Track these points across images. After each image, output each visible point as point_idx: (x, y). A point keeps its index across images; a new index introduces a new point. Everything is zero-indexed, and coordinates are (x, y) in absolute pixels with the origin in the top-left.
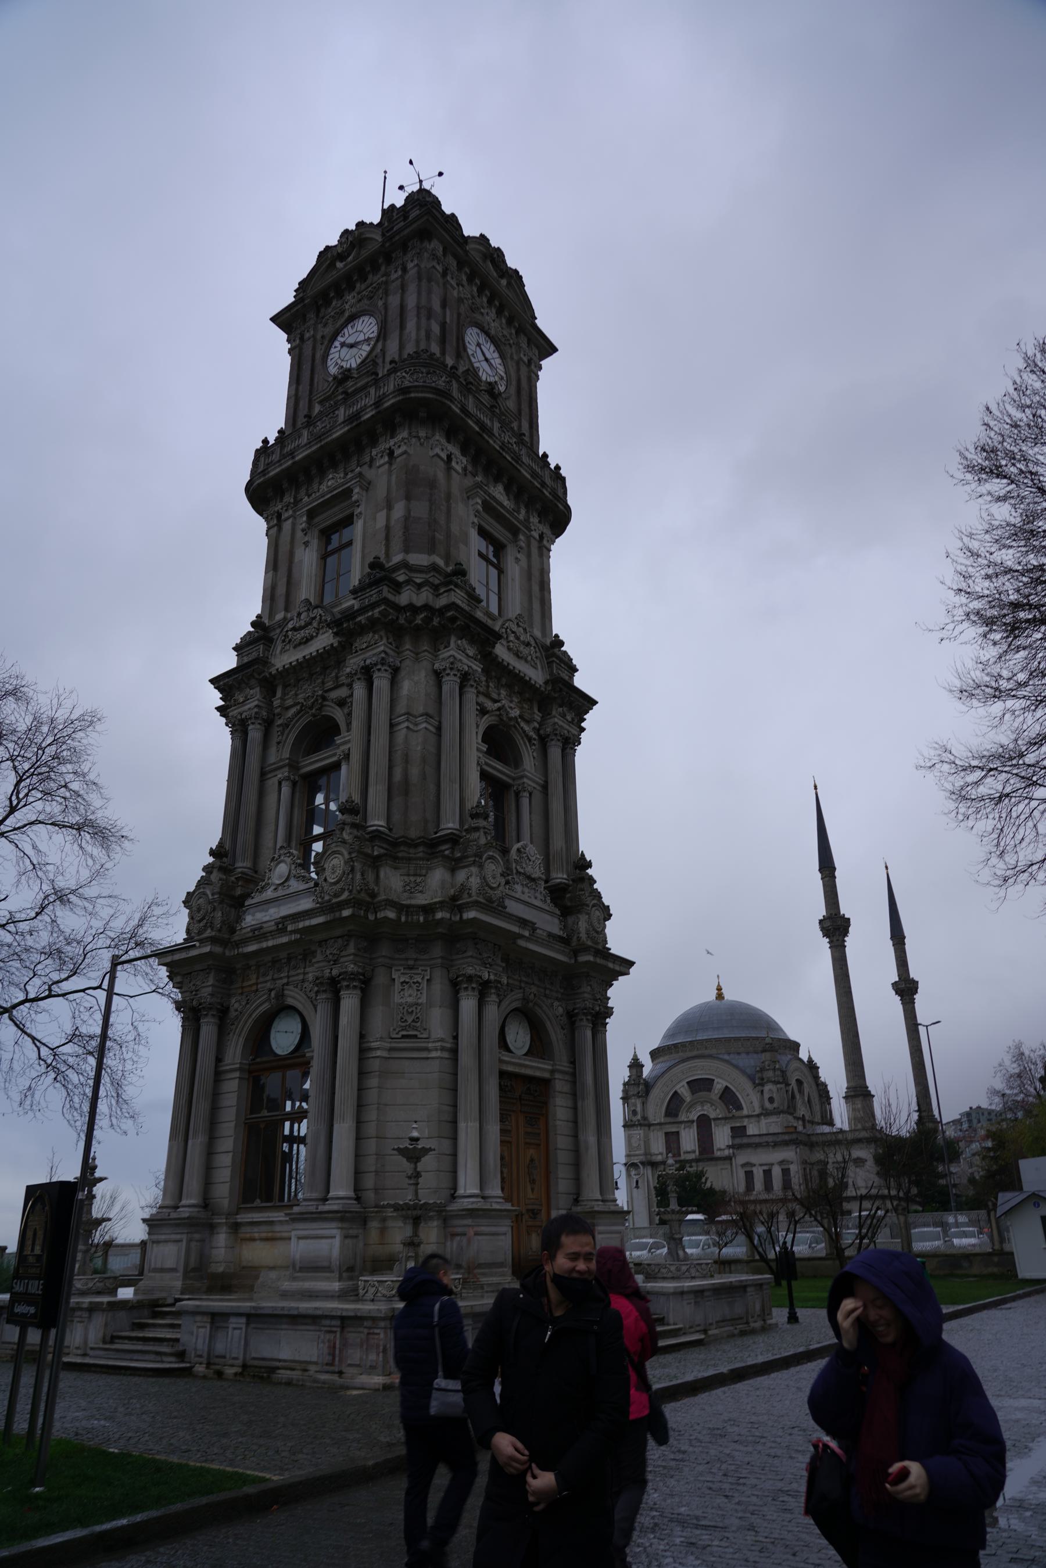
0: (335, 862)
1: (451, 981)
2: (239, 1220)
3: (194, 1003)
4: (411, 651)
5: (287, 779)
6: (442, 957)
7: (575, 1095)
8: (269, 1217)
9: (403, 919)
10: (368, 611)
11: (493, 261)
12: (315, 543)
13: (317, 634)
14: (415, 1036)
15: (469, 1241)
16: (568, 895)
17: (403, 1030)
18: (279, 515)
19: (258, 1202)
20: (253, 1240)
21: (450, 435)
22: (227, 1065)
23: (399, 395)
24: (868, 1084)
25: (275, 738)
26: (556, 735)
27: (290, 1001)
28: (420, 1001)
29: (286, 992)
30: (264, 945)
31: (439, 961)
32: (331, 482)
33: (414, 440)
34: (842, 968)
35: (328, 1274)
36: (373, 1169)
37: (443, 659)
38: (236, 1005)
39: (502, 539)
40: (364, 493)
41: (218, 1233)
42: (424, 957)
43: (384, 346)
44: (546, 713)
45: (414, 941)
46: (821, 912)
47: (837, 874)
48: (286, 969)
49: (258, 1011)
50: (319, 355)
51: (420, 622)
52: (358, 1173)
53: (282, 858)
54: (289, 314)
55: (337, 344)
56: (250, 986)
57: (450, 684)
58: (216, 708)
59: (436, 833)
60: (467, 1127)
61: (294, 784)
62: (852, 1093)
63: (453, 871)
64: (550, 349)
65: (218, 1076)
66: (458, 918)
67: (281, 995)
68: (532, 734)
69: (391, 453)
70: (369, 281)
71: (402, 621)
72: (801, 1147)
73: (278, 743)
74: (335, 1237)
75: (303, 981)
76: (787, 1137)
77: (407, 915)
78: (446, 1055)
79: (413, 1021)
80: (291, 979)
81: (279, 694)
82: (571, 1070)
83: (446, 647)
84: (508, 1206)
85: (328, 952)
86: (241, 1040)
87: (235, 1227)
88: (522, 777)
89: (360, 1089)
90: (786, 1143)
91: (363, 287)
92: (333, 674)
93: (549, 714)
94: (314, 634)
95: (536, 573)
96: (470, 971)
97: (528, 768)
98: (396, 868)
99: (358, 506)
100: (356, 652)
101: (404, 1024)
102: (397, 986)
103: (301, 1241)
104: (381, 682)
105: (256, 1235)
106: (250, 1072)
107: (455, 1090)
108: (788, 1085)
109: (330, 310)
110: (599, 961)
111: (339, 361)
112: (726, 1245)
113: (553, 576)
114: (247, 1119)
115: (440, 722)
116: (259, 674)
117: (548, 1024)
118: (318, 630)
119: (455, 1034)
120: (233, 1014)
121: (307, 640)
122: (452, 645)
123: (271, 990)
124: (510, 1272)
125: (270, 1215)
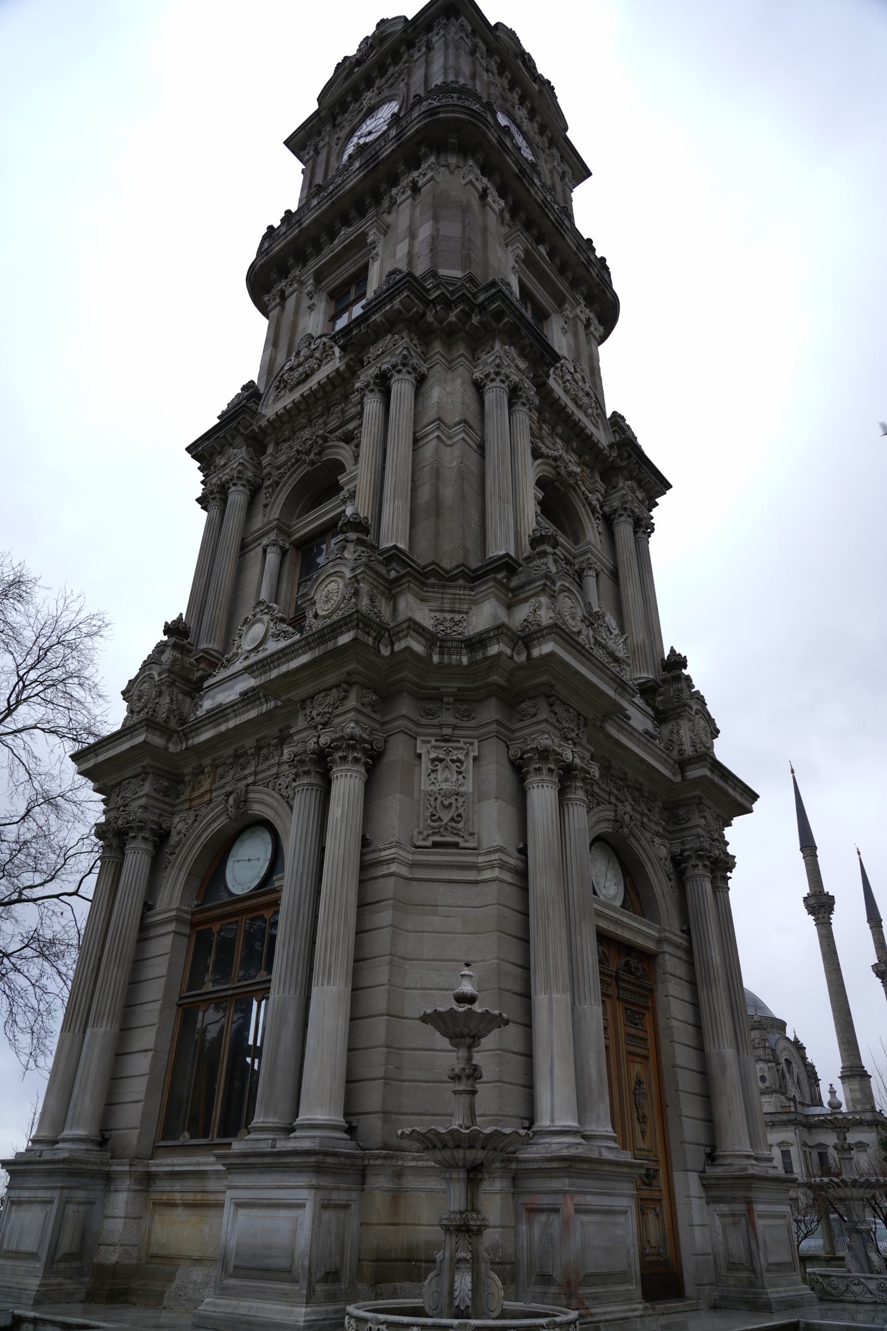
0: (333, 586)
1: (512, 763)
2: (153, 1169)
3: (120, 822)
4: (442, 356)
5: (274, 544)
6: (498, 722)
8: (199, 1164)
9: (436, 659)
10: (385, 305)
11: (524, 62)
13: (320, 366)
14: (455, 845)
15: (566, 1224)
16: (659, 699)
17: (434, 833)
19: (185, 1138)
20: (172, 1205)
21: (486, 170)
22: (158, 914)
23: (425, 118)
24: (864, 1064)
25: (262, 499)
26: (625, 509)
27: (257, 809)
28: (462, 789)
29: (251, 795)
30: (223, 728)
31: (494, 727)
32: (346, 234)
33: (442, 169)
34: (829, 946)
35: (286, 1286)
36: (380, 1072)
38: (180, 826)
39: (544, 303)
40: (382, 237)
41: (116, 1191)
42: (469, 724)
44: (611, 487)
45: (451, 699)
46: (805, 889)
47: (818, 853)
48: (253, 763)
49: (209, 831)
51: (454, 319)
52: (352, 1081)
53: (258, 616)
54: (303, 132)
56: (202, 796)
57: (496, 395)
60: (550, 1000)
61: (284, 553)
62: (848, 1073)
63: (510, 607)
65: (145, 931)
66: (523, 657)
67: (243, 802)
70: (390, 73)
71: (430, 318)
72: (801, 1128)
73: (266, 506)
74: (301, 1206)
75: (277, 776)
76: (784, 1117)
77: (441, 653)
78: (507, 877)
79: (452, 819)
80: (259, 777)
81: (270, 449)
82: (685, 943)
84: (626, 1156)
85: (314, 713)
86: (183, 876)
87: (148, 1179)
88: (585, 553)
89: (360, 932)
90: (785, 1124)
93: (614, 488)
94: (316, 366)
96: (545, 741)
97: (593, 541)
98: (423, 600)
99: (374, 248)
100: (369, 362)
101: (436, 824)
102: (425, 763)
103: (241, 1211)
105: (178, 1197)
106: (193, 925)
107: (525, 940)
108: (778, 1064)
109: (346, 115)
110: (717, 780)
112: (805, 1237)
113: (602, 364)
114: (181, 998)
115: (483, 440)
116: (246, 429)
117: (649, 868)
118: (321, 361)
119: (521, 845)
120: (174, 838)
121: (307, 376)
123: (228, 795)
124: (639, 1292)
125: (201, 1159)
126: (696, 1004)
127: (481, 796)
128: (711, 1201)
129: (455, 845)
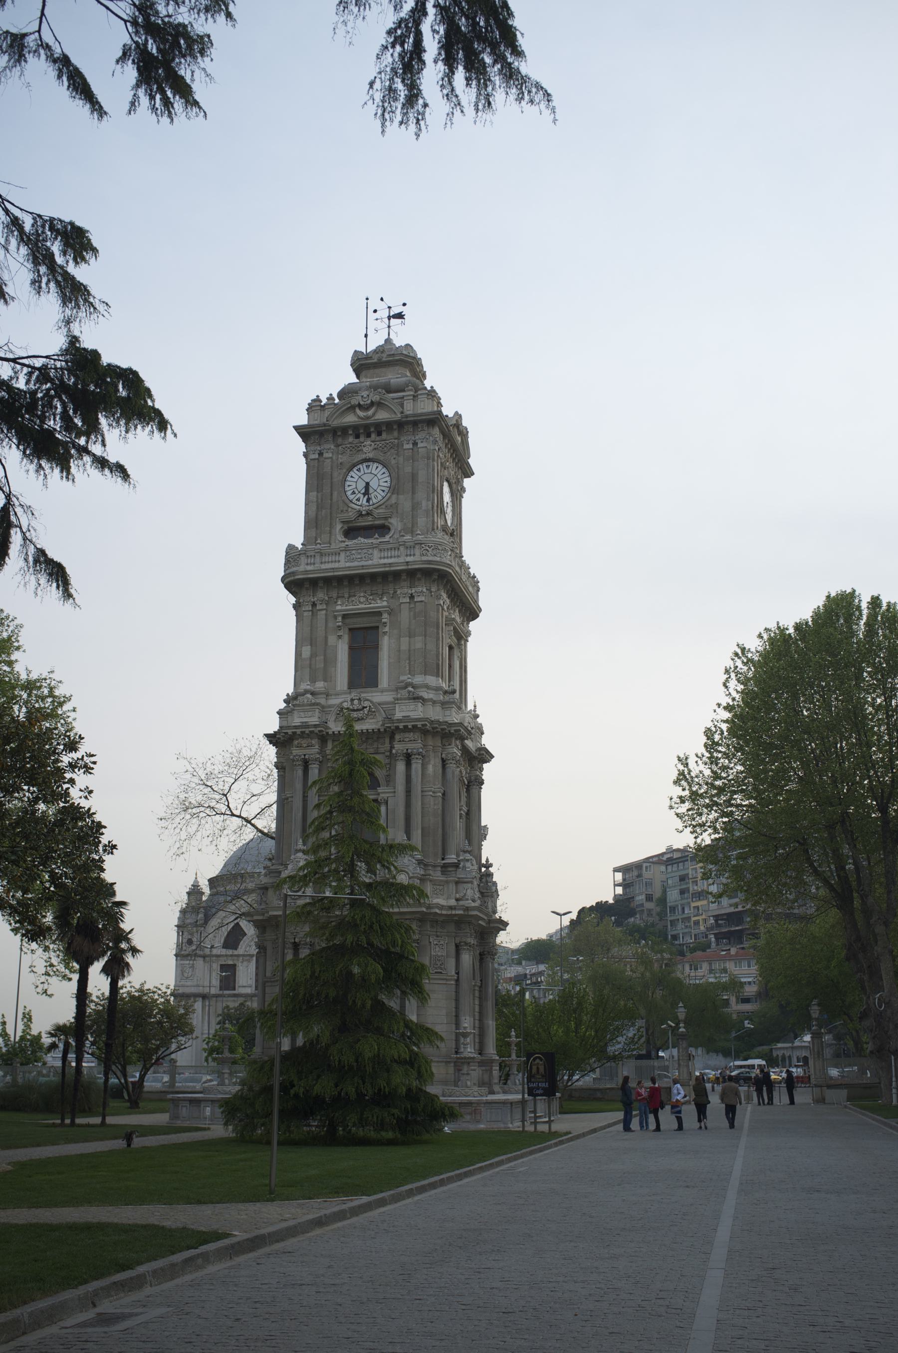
1: (456, 944)
12: (346, 638)
14: (441, 973)
18: (314, 605)
37: (449, 753)
42: (445, 931)
43: (397, 499)
50: (337, 476)
55: (352, 473)
57: (451, 766)
59: (443, 859)
64: (469, 473)
68: (466, 782)
69: (412, 597)
83: (450, 745)
91: (378, 438)
92: (375, 746)
104: (416, 766)
107: (457, 1000)
111: (357, 492)
126: (480, 1006)
127: (448, 956)
129: (441, 973)
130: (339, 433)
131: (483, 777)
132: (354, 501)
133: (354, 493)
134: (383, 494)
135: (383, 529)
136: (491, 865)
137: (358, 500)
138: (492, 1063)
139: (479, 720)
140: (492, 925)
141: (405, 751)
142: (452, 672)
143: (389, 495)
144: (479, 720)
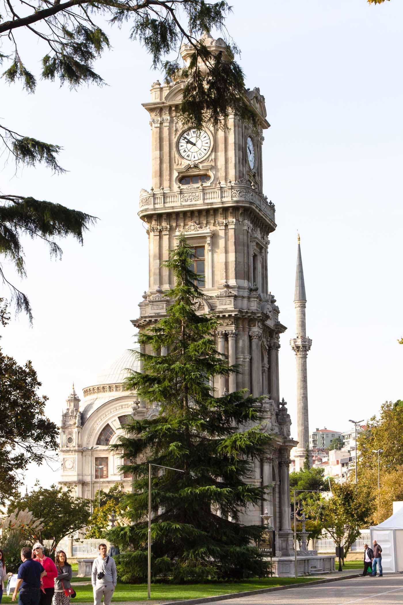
7: (280, 493)
14: (251, 478)
18: (160, 232)
23: (234, 203)
57: (255, 341)
58: (131, 321)
68: (267, 348)
95: (265, 266)
111: (187, 151)
115: (251, 357)
122: (256, 325)
126: (280, 498)
128: (279, 538)
129: (251, 478)
130: (173, 109)
131: (280, 343)
132: (185, 157)
133: (185, 151)
134: (205, 152)
135: (205, 177)
136: (286, 403)
137: (188, 156)
138: (288, 535)
139: (276, 304)
140: (286, 444)
141: (224, 332)
142: (256, 272)
143: (209, 152)
144: (276, 304)
